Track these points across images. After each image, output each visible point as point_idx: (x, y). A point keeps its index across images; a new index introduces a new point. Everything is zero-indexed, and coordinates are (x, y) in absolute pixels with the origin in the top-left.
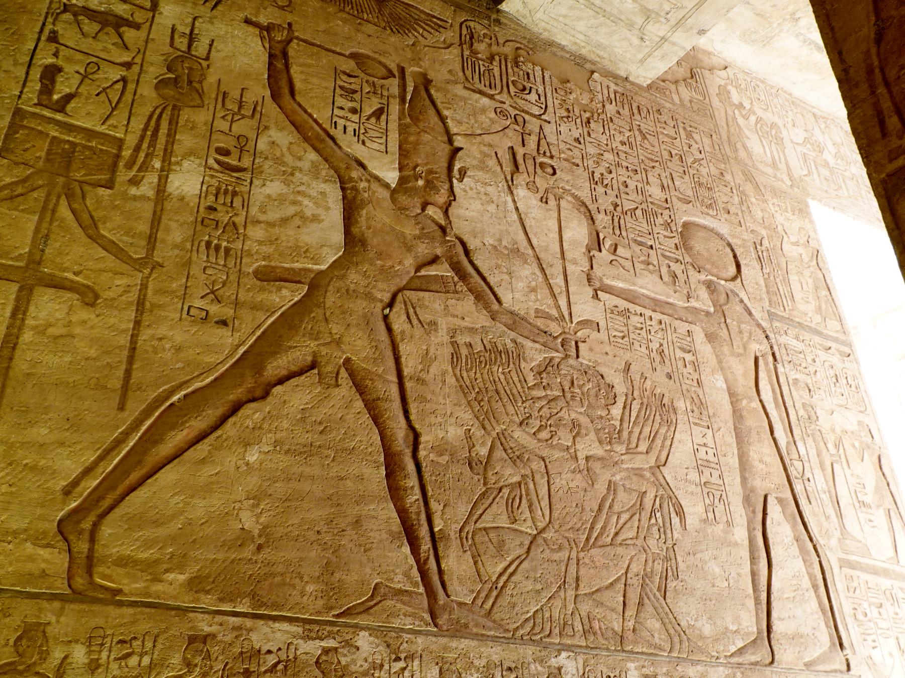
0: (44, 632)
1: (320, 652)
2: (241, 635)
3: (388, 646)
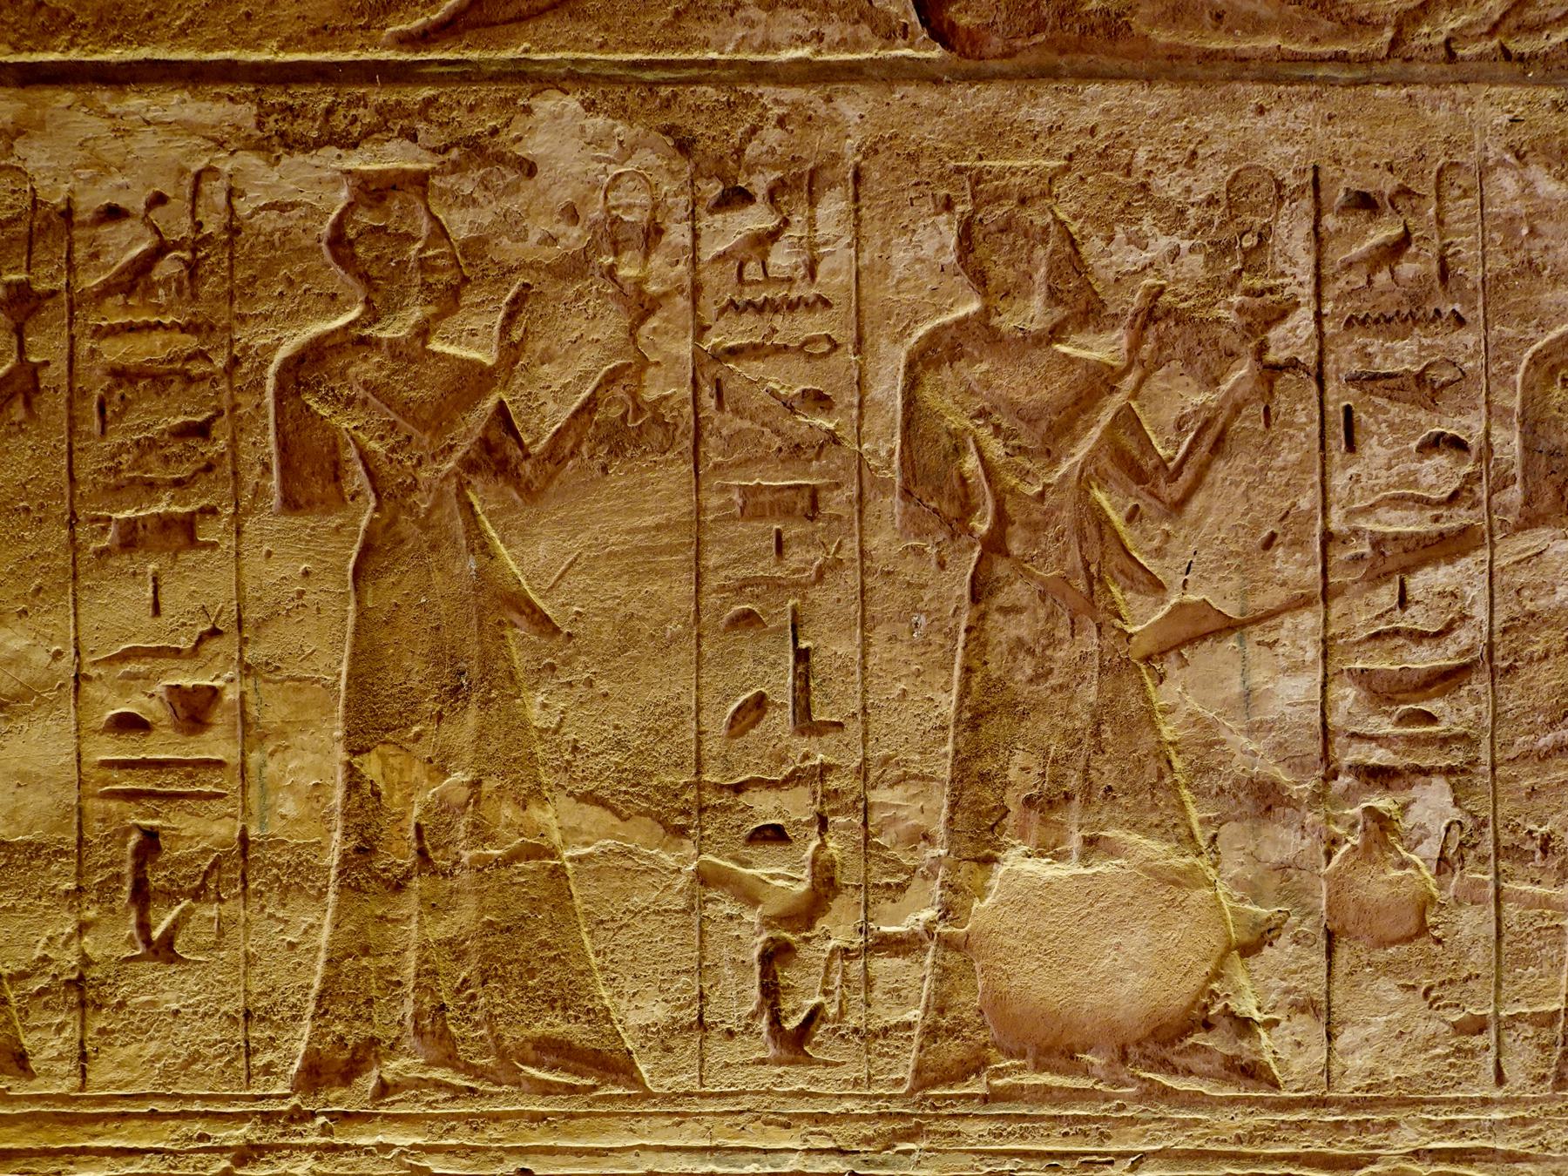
1: (344, 196)
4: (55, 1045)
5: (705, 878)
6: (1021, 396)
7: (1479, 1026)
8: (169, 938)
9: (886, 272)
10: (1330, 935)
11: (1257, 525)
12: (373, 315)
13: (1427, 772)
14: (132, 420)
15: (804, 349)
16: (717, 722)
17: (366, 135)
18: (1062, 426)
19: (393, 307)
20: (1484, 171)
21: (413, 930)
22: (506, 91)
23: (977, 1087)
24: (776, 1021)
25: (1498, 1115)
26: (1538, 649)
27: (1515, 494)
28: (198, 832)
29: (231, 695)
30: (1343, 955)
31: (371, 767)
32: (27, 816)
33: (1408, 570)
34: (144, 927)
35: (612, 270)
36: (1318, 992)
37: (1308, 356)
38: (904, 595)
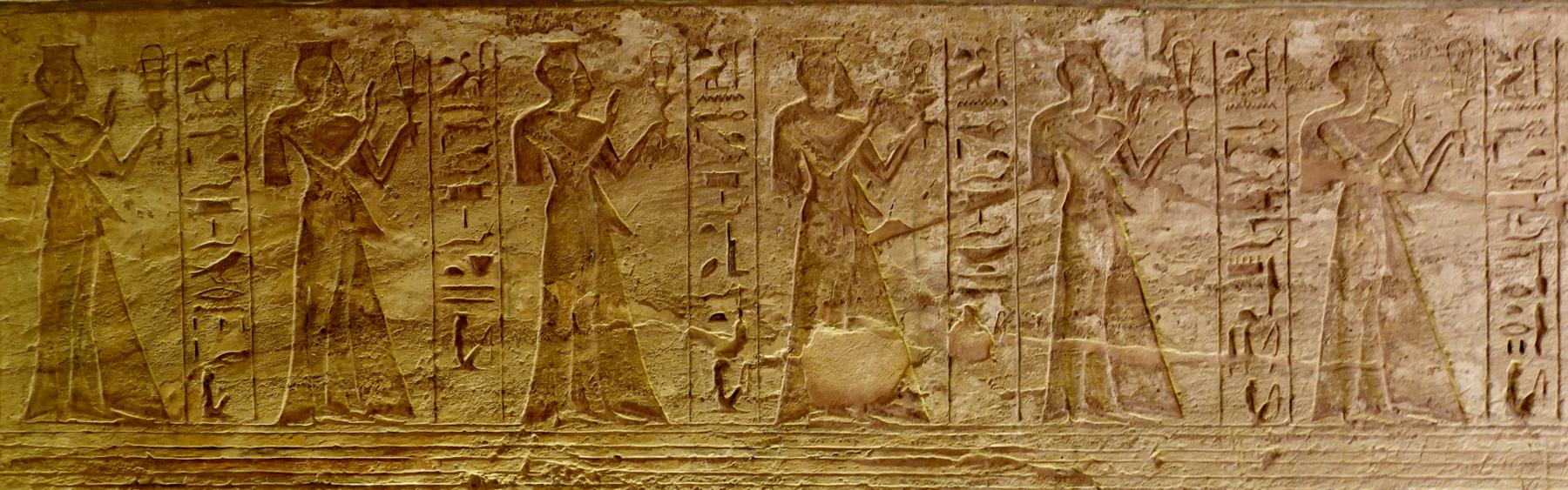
0: (74, 59)
1: (543, 53)
2: (392, 37)
3: (684, 32)
4: (425, 404)
5: (692, 335)
6: (824, 136)
7: (1012, 396)
8: (471, 360)
9: (767, 83)
10: (950, 359)
11: (920, 189)
12: (554, 103)
13: (991, 291)
14: (456, 146)
15: (733, 116)
16: (697, 271)
17: (551, 28)
18: (841, 148)
19: (563, 100)
20: (1016, 41)
21: (571, 357)
22: (609, 9)
23: (804, 421)
24: (721, 395)
25: (1019, 433)
26: (1037, 240)
27: (1028, 175)
28: (483, 316)
29: (496, 260)
30: (955, 367)
31: (554, 290)
32: (413, 309)
33: (982, 207)
34: (461, 355)
35: (653, 84)
36: (945, 382)
37: (942, 119)
38: (774, 219)
